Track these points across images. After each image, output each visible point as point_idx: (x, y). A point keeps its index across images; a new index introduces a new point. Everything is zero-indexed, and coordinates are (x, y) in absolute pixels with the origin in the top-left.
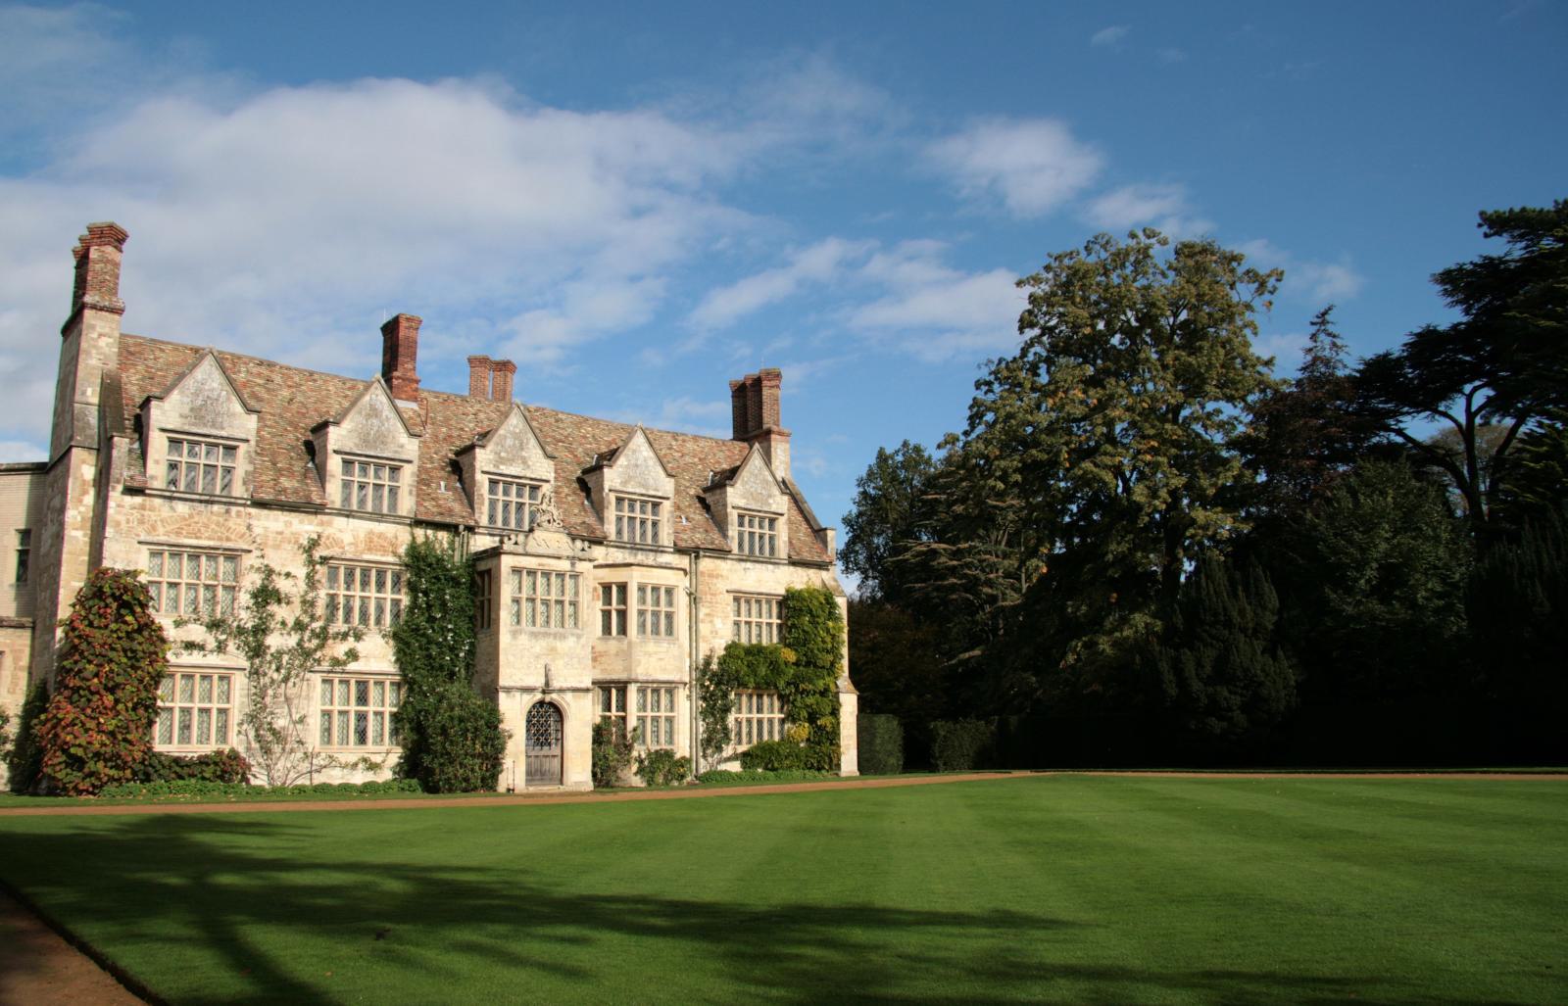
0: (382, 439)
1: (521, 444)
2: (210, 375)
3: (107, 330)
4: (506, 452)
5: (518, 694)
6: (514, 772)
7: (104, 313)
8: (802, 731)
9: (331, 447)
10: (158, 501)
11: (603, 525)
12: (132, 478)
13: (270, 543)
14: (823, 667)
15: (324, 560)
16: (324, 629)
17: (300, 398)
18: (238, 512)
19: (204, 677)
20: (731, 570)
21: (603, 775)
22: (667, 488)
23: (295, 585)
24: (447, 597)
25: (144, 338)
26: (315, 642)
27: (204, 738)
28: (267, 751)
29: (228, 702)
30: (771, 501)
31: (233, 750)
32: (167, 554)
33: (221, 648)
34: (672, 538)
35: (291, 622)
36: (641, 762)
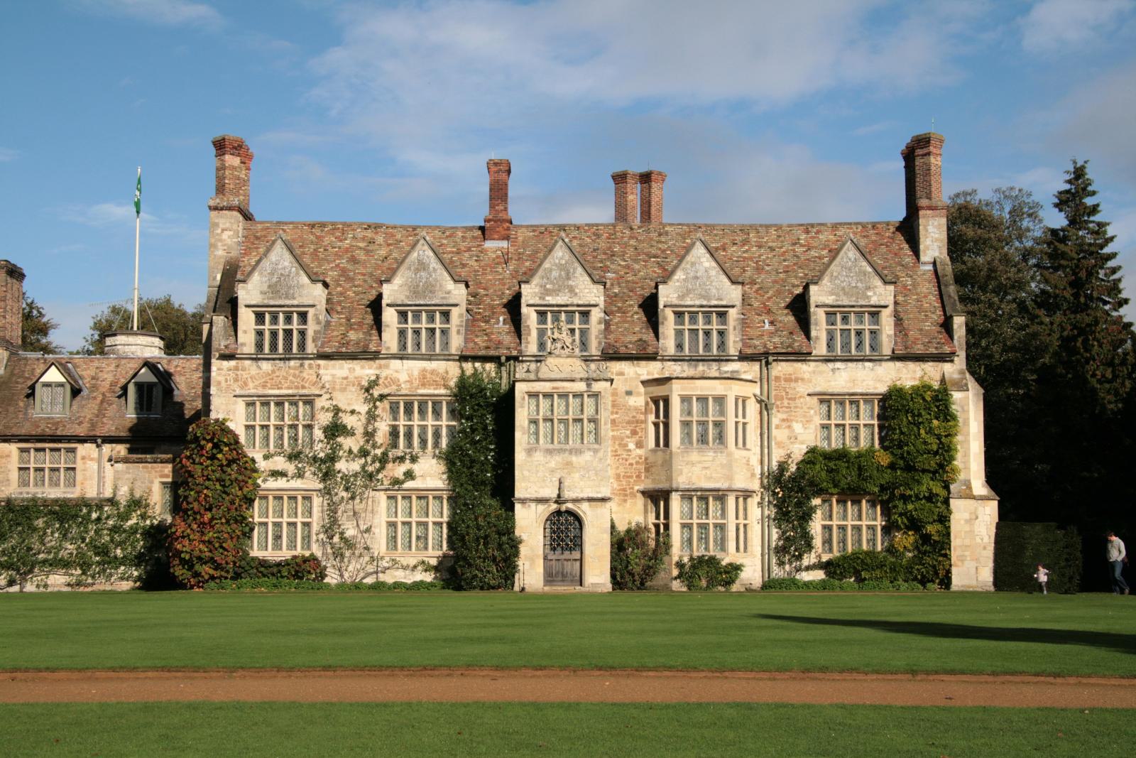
0: (430, 288)
1: (568, 274)
2: (281, 256)
3: (228, 225)
4: (552, 283)
5: (533, 505)
6: (531, 571)
7: (224, 212)
8: (905, 540)
9: (384, 302)
10: (247, 363)
11: (658, 340)
12: (226, 347)
13: (338, 387)
14: (924, 471)
15: (382, 397)
16: (385, 454)
17: (395, 255)
18: (310, 364)
19: (290, 498)
20: (814, 372)
21: (622, 577)
22: (733, 296)
23: (360, 420)
24: (488, 422)
25: (271, 222)
26: (377, 465)
27: (292, 545)
28: (338, 554)
29: (311, 517)
30: (870, 294)
31: (312, 555)
32: (258, 404)
33: (300, 475)
34: (739, 345)
35: (355, 450)
36: (680, 565)
